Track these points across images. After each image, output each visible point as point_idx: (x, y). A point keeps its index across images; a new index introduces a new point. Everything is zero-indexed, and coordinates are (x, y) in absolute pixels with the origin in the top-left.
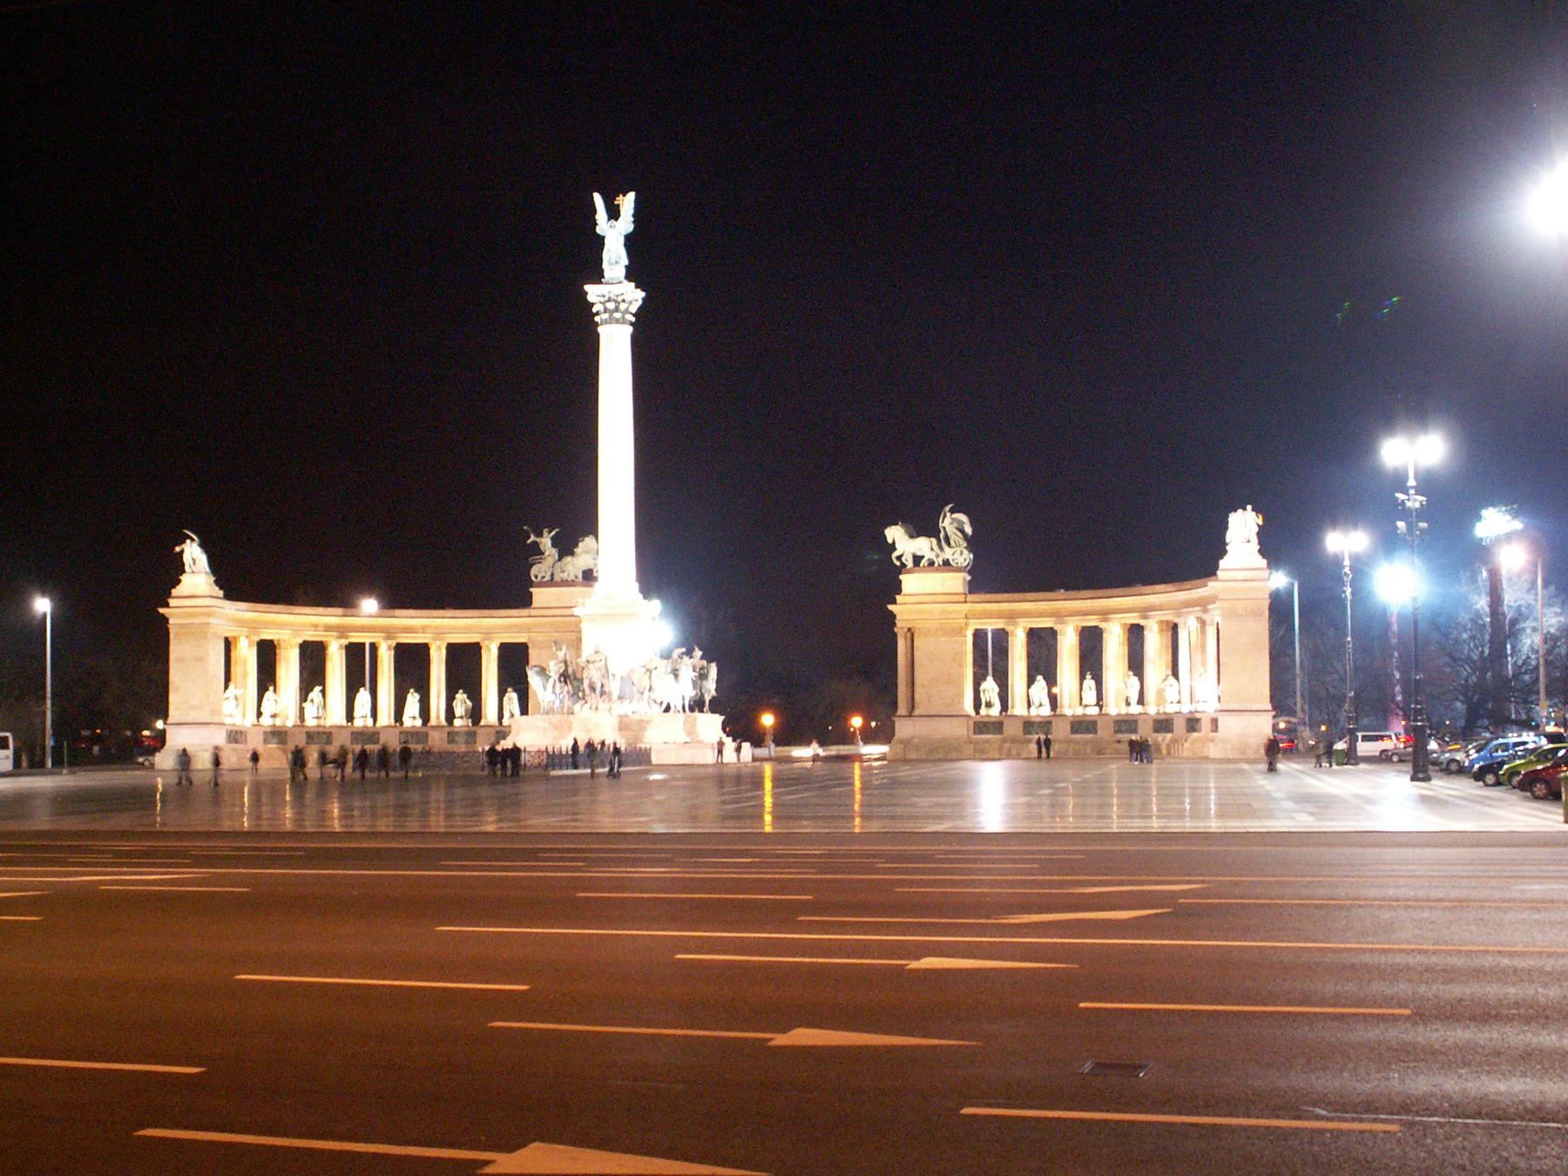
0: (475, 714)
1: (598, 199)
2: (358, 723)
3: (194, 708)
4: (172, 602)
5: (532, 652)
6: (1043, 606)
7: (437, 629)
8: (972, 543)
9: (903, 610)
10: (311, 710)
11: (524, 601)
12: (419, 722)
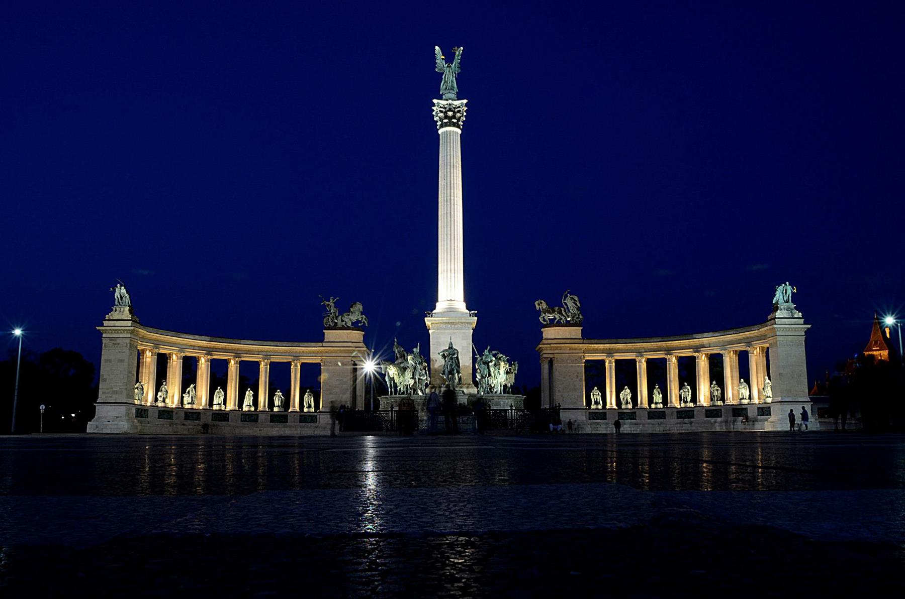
0: (286, 404)
2: (215, 408)
3: (116, 392)
4: (105, 323)
7: (264, 353)
9: (546, 349)
10: (187, 399)
11: (320, 339)
12: (253, 409)
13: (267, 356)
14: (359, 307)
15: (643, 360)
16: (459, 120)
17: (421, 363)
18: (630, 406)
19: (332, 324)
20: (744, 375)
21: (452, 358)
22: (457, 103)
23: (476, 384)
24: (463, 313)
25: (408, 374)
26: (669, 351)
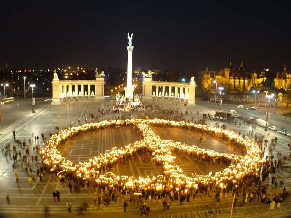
1: (128, 34)
11: (95, 80)
14: (103, 72)
20: (184, 92)
26: (170, 85)
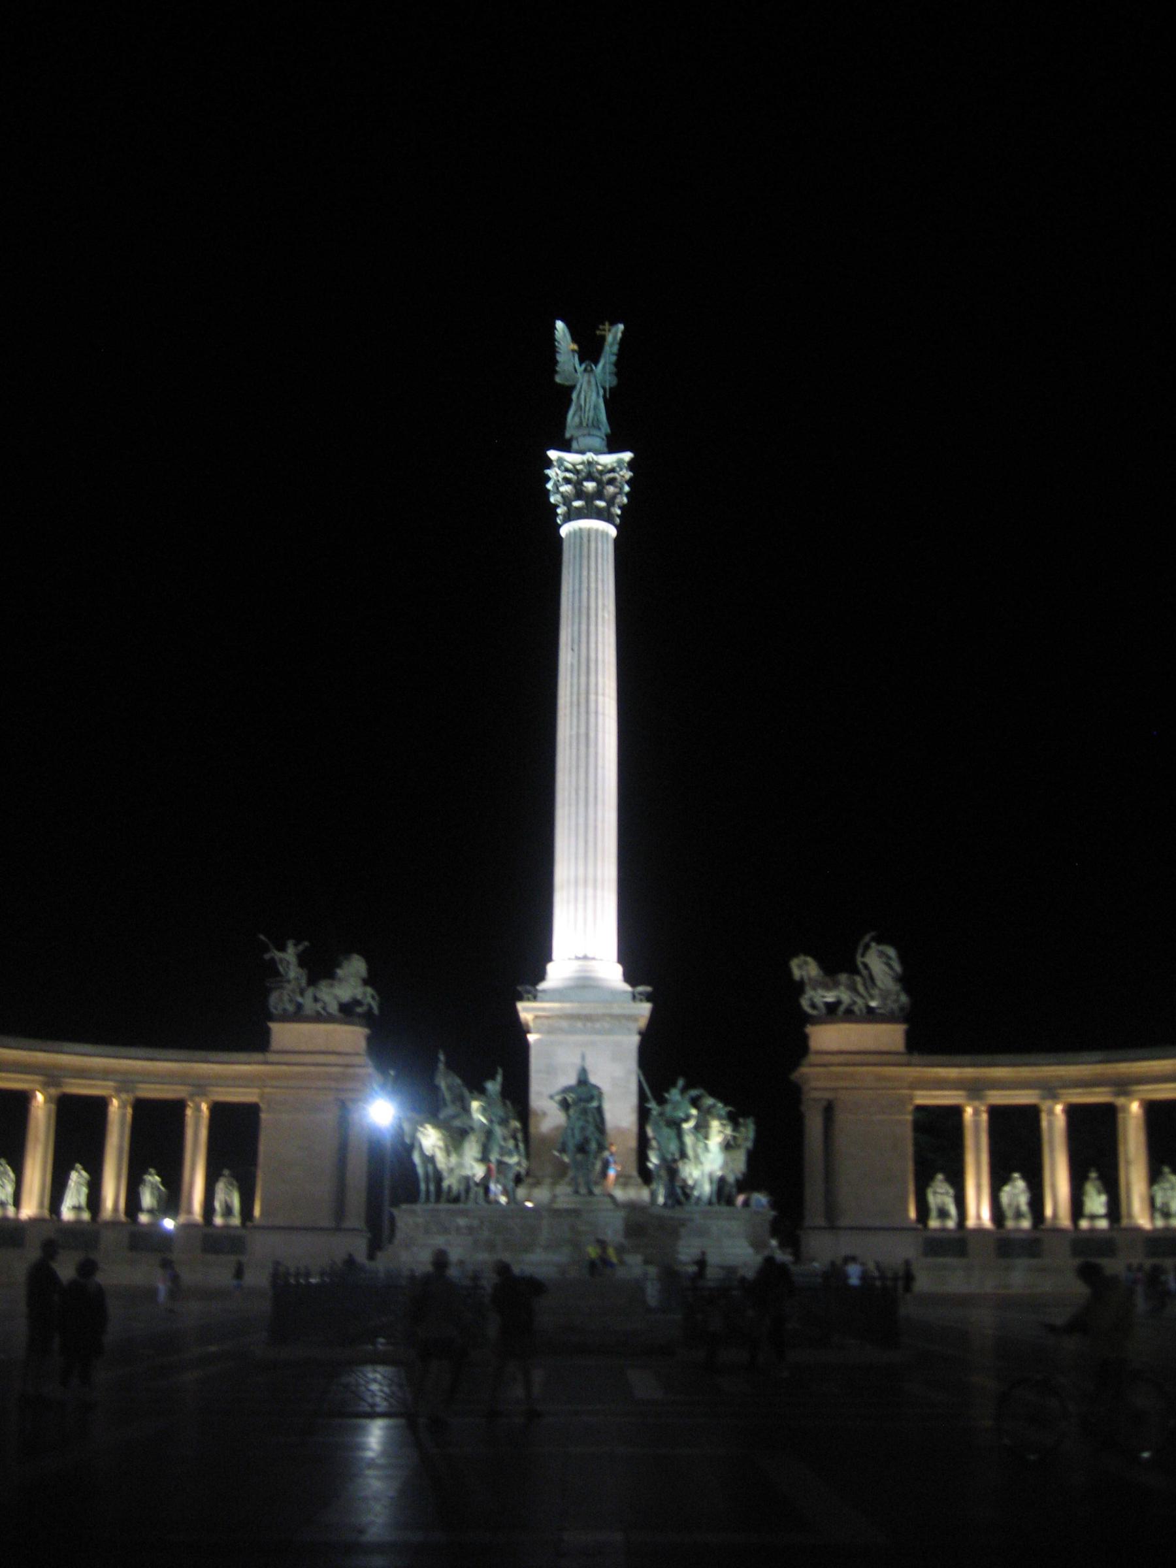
5: (263, 1116)
6: (1025, 1072)
7: (118, 1077)
8: (906, 981)
9: (813, 1077)
12: (86, 1216)
13: (125, 1083)
14: (355, 967)
15: (1059, 1108)
16: (611, 502)
17: (504, 1122)
18: (1026, 1224)
19: (291, 1008)
21: (585, 1112)
22: (608, 460)
23: (646, 1176)
24: (614, 993)
25: (472, 1149)
26: (1123, 1086)
